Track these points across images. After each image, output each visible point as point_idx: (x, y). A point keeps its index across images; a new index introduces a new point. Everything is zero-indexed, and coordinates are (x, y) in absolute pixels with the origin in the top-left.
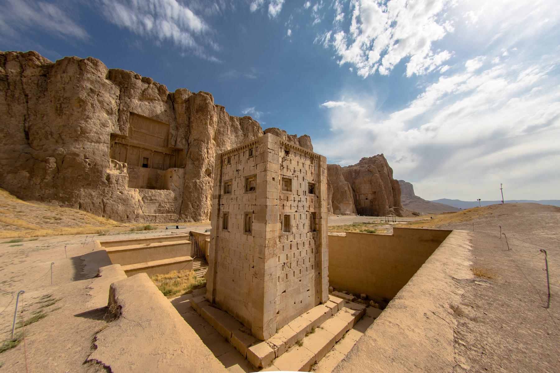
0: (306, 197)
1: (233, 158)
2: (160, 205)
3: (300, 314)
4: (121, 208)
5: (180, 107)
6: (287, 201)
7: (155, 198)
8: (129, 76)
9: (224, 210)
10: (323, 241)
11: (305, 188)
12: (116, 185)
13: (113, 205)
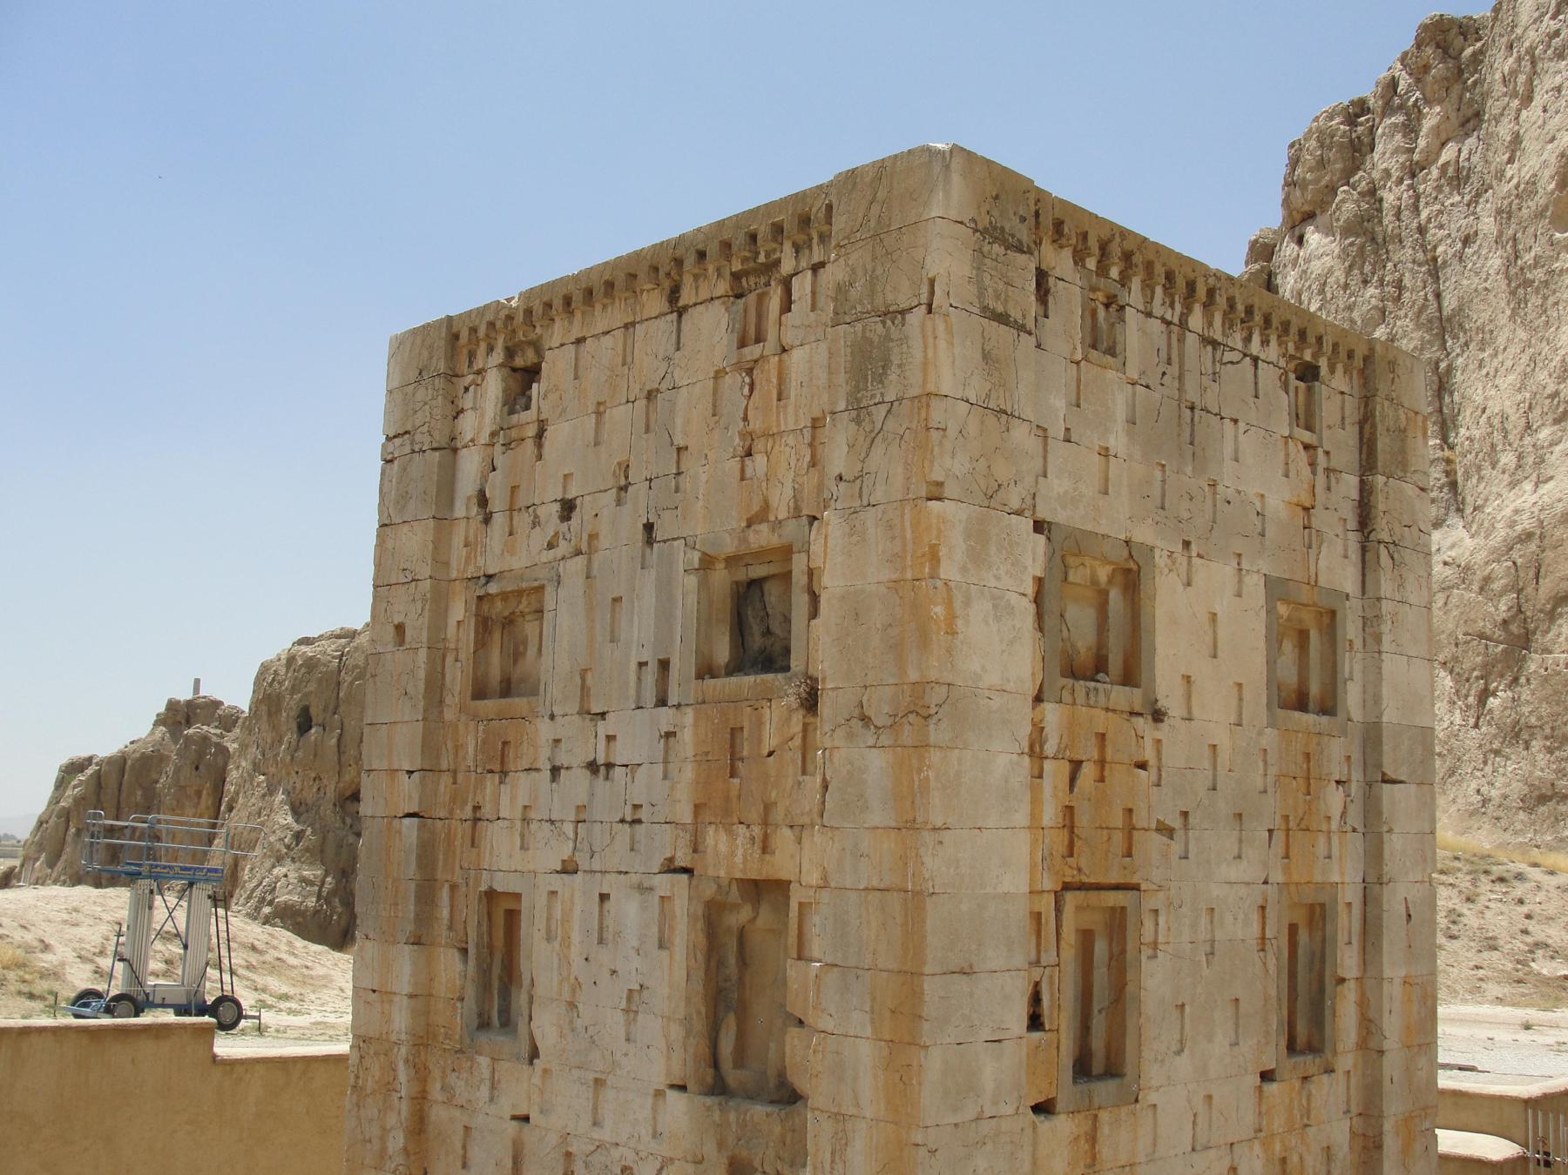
0: (666, 717)
6: (504, 773)
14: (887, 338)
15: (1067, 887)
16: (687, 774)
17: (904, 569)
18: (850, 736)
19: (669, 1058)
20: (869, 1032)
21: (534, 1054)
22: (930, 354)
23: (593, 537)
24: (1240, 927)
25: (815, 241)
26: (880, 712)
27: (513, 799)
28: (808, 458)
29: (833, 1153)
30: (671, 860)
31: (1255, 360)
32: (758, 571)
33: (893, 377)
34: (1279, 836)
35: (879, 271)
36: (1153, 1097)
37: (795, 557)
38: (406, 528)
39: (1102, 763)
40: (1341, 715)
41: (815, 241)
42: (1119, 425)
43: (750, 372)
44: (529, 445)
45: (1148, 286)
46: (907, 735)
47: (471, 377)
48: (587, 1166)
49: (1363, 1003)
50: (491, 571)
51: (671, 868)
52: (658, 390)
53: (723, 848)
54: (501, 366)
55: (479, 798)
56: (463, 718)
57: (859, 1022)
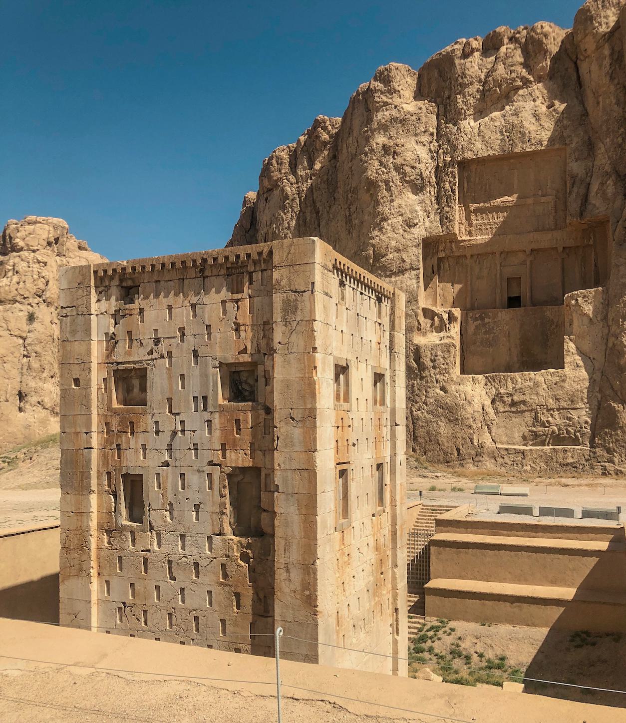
0: (207, 416)
2: (536, 418)
4: (444, 429)
5: (594, 67)
7: (522, 398)
8: (449, 59)
10: (280, 575)
12: (432, 371)
13: (428, 422)
14: (296, 300)
15: (338, 464)
16: (217, 434)
17: (305, 373)
18: (286, 424)
19: (213, 525)
20: (297, 512)
21: (152, 528)
22: (313, 307)
23: (169, 353)
24: (368, 472)
25: (262, 261)
26: (298, 415)
28: (262, 335)
29: (285, 550)
31: (370, 297)
32: (238, 369)
33: (299, 313)
34: (374, 443)
35: (292, 278)
36: (353, 525)
37: (259, 366)
39: (342, 426)
40: (386, 405)
41: (262, 261)
42: (345, 324)
43: (237, 303)
45: (350, 278)
46: (308, 424)
47: (103, 288)
48: (178, 564)
49: (391, 491)
51: (211, 463)
52: (196, 304)
54: (117, 286)
55: (119, 442)
56: (109, 413)
57: (293, 509)
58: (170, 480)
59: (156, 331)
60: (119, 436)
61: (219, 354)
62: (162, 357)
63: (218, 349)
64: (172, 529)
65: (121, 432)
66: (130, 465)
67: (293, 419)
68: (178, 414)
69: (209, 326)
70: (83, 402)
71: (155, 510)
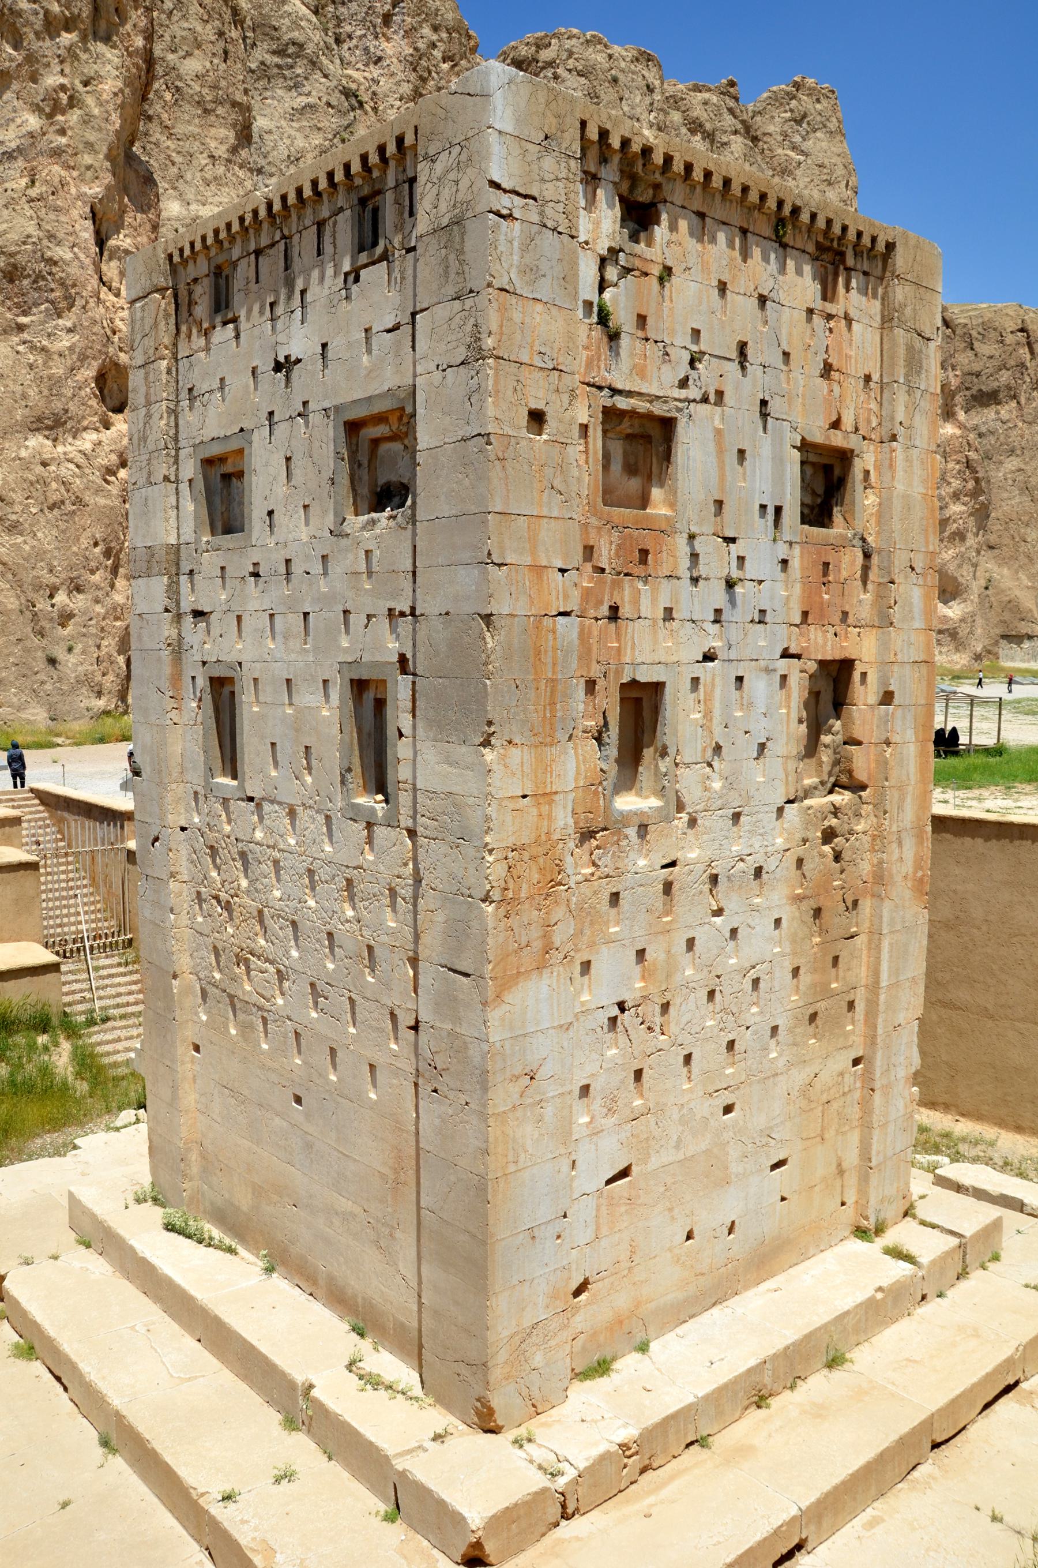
1: (244, 270)
3: (717, 1291)
9: (210, 650)
11: (778, 479)
16: (797, 589)
19: (787, 784)
21: (680, 807)
27: (654, 601)
30: (786, 649)
38: (539, 307)
44: (654, 282)
48: (729, 877)
50: (619, 386)
51: (786, 654)
53: (820, 641)
58: (718, 692)
59: (696, 333)
60: (617, 585)
61: (800, 421)
62: (705, 400)
63: (800, 408)
64: (719, 803)
65: (619, 574)
66: (639, 660)
67: (913, 569)
68: (733, 540)
69: (786, 355)
70: (556, 484)
71: (687, 765)
